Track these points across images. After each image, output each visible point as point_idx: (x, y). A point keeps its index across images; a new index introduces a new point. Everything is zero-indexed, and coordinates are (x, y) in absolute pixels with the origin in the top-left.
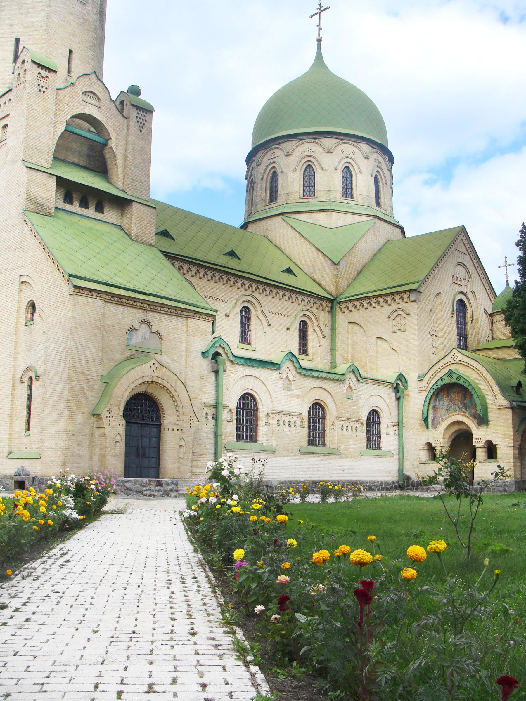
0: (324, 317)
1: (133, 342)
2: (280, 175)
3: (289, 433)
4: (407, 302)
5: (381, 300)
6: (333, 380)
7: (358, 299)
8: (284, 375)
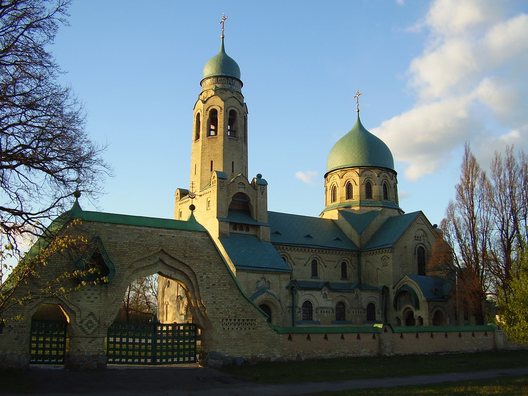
2: (337, 188)
3: (326, 316)
4: (388, 253)
5: (378, 251)
6: (348, 292)
8: (324, 292)
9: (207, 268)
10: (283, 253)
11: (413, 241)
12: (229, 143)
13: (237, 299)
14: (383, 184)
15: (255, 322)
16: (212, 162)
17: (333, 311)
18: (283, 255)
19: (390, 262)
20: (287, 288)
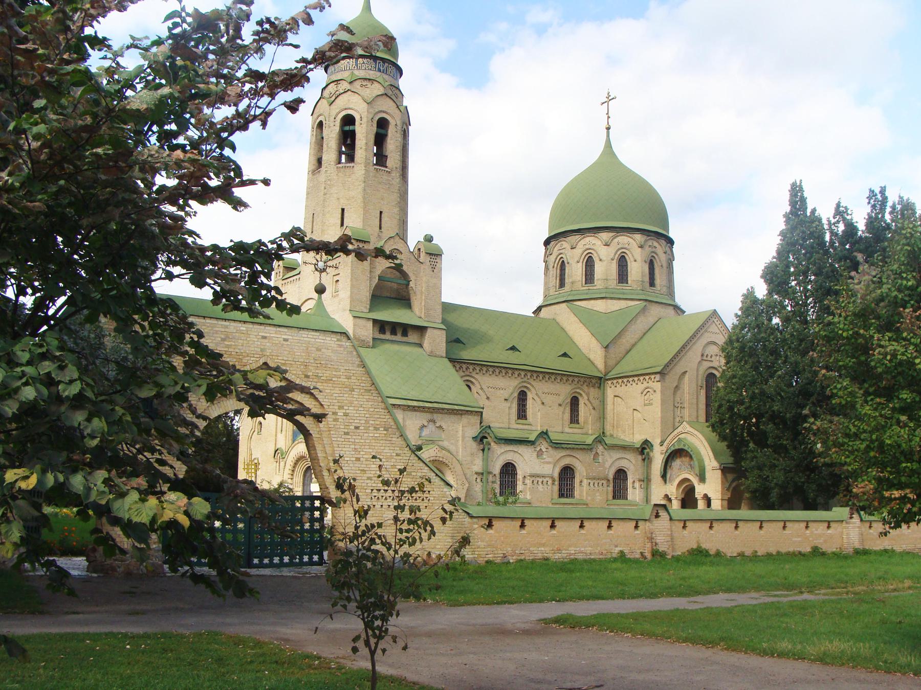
0: (594, 392)
1: (424, 434)
2: (566, 264)
3: (541, 490)
6: (581, 449)
7: (620, 378)
8: (538, 449)
9: (345, 398)
10: (468, 378)
11: (700, 362)
12: (375, 176)
13: (397, 455)
14: (648, 261)
15: (428, 496)
16: (343, 210)
17: (554, 481)
18: (468, 380)
19: (657, 398)
20: (474, 438)
